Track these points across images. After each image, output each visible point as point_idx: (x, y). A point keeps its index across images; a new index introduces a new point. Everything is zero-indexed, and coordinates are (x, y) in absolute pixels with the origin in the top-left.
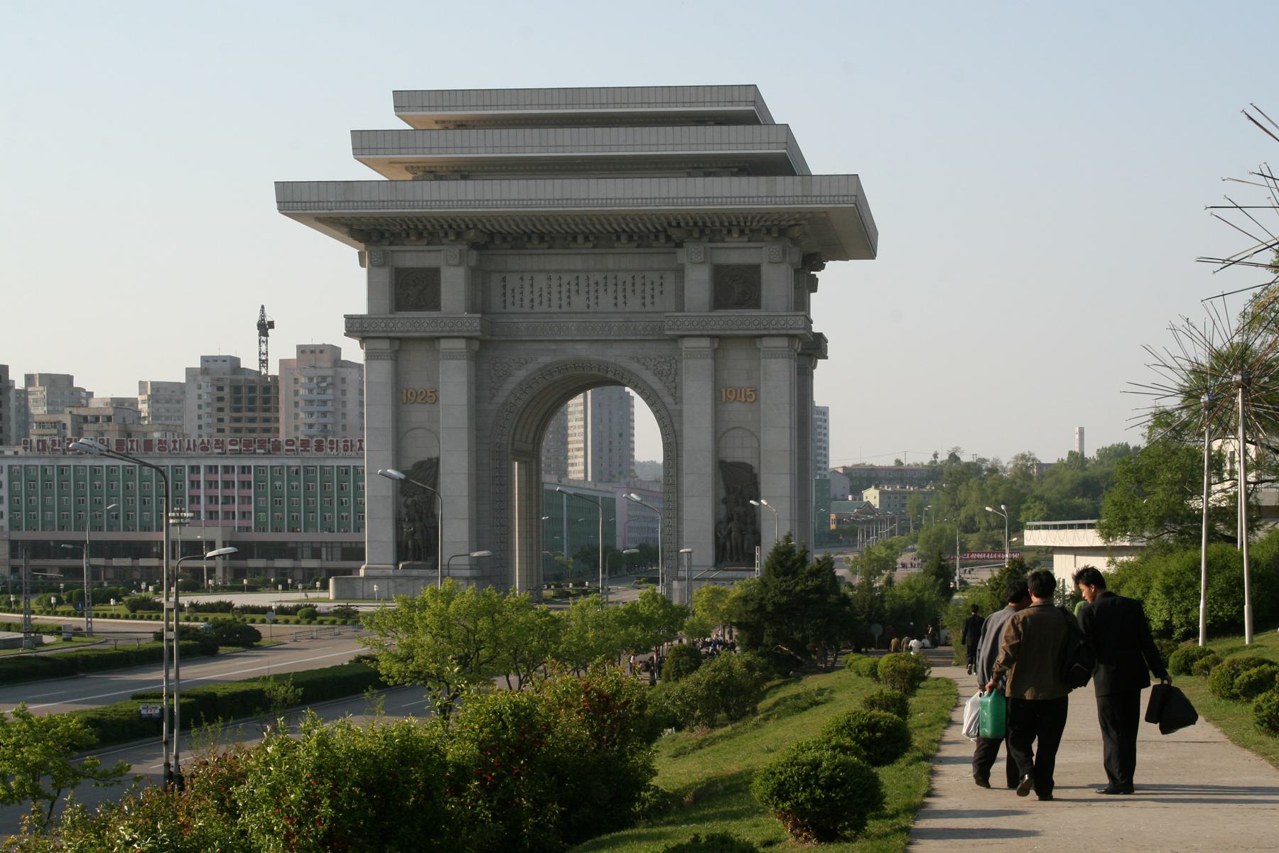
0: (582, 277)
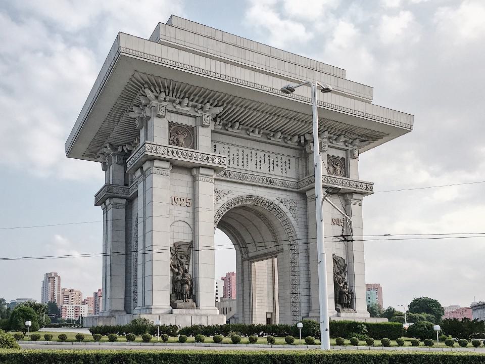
0: (254, 152)
